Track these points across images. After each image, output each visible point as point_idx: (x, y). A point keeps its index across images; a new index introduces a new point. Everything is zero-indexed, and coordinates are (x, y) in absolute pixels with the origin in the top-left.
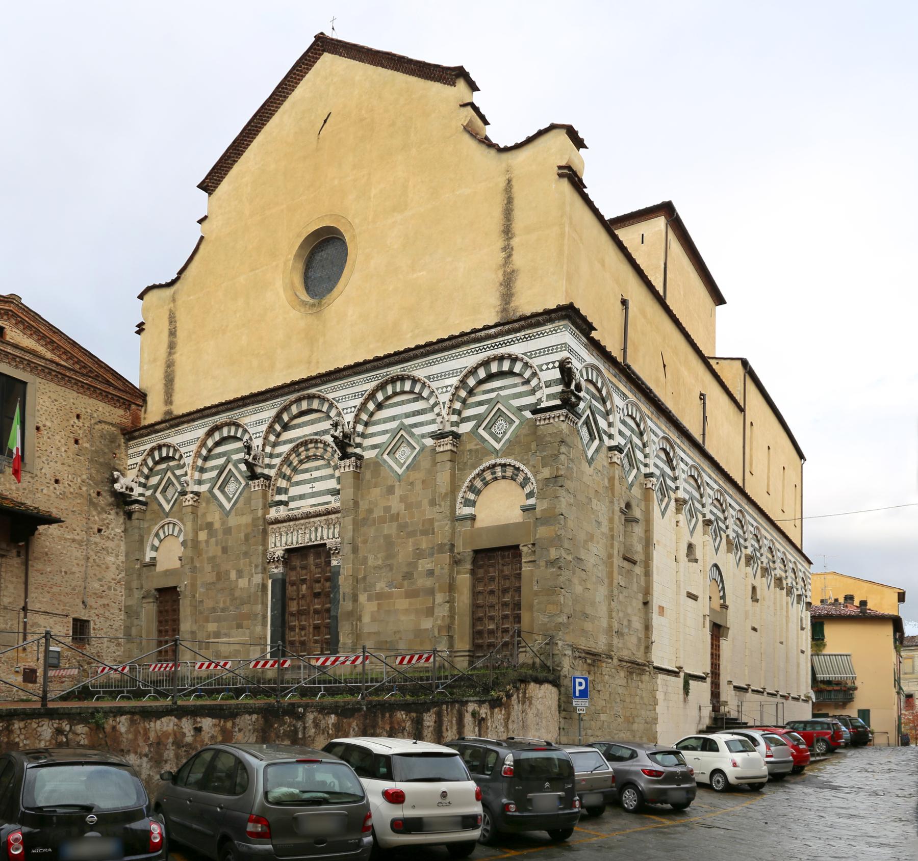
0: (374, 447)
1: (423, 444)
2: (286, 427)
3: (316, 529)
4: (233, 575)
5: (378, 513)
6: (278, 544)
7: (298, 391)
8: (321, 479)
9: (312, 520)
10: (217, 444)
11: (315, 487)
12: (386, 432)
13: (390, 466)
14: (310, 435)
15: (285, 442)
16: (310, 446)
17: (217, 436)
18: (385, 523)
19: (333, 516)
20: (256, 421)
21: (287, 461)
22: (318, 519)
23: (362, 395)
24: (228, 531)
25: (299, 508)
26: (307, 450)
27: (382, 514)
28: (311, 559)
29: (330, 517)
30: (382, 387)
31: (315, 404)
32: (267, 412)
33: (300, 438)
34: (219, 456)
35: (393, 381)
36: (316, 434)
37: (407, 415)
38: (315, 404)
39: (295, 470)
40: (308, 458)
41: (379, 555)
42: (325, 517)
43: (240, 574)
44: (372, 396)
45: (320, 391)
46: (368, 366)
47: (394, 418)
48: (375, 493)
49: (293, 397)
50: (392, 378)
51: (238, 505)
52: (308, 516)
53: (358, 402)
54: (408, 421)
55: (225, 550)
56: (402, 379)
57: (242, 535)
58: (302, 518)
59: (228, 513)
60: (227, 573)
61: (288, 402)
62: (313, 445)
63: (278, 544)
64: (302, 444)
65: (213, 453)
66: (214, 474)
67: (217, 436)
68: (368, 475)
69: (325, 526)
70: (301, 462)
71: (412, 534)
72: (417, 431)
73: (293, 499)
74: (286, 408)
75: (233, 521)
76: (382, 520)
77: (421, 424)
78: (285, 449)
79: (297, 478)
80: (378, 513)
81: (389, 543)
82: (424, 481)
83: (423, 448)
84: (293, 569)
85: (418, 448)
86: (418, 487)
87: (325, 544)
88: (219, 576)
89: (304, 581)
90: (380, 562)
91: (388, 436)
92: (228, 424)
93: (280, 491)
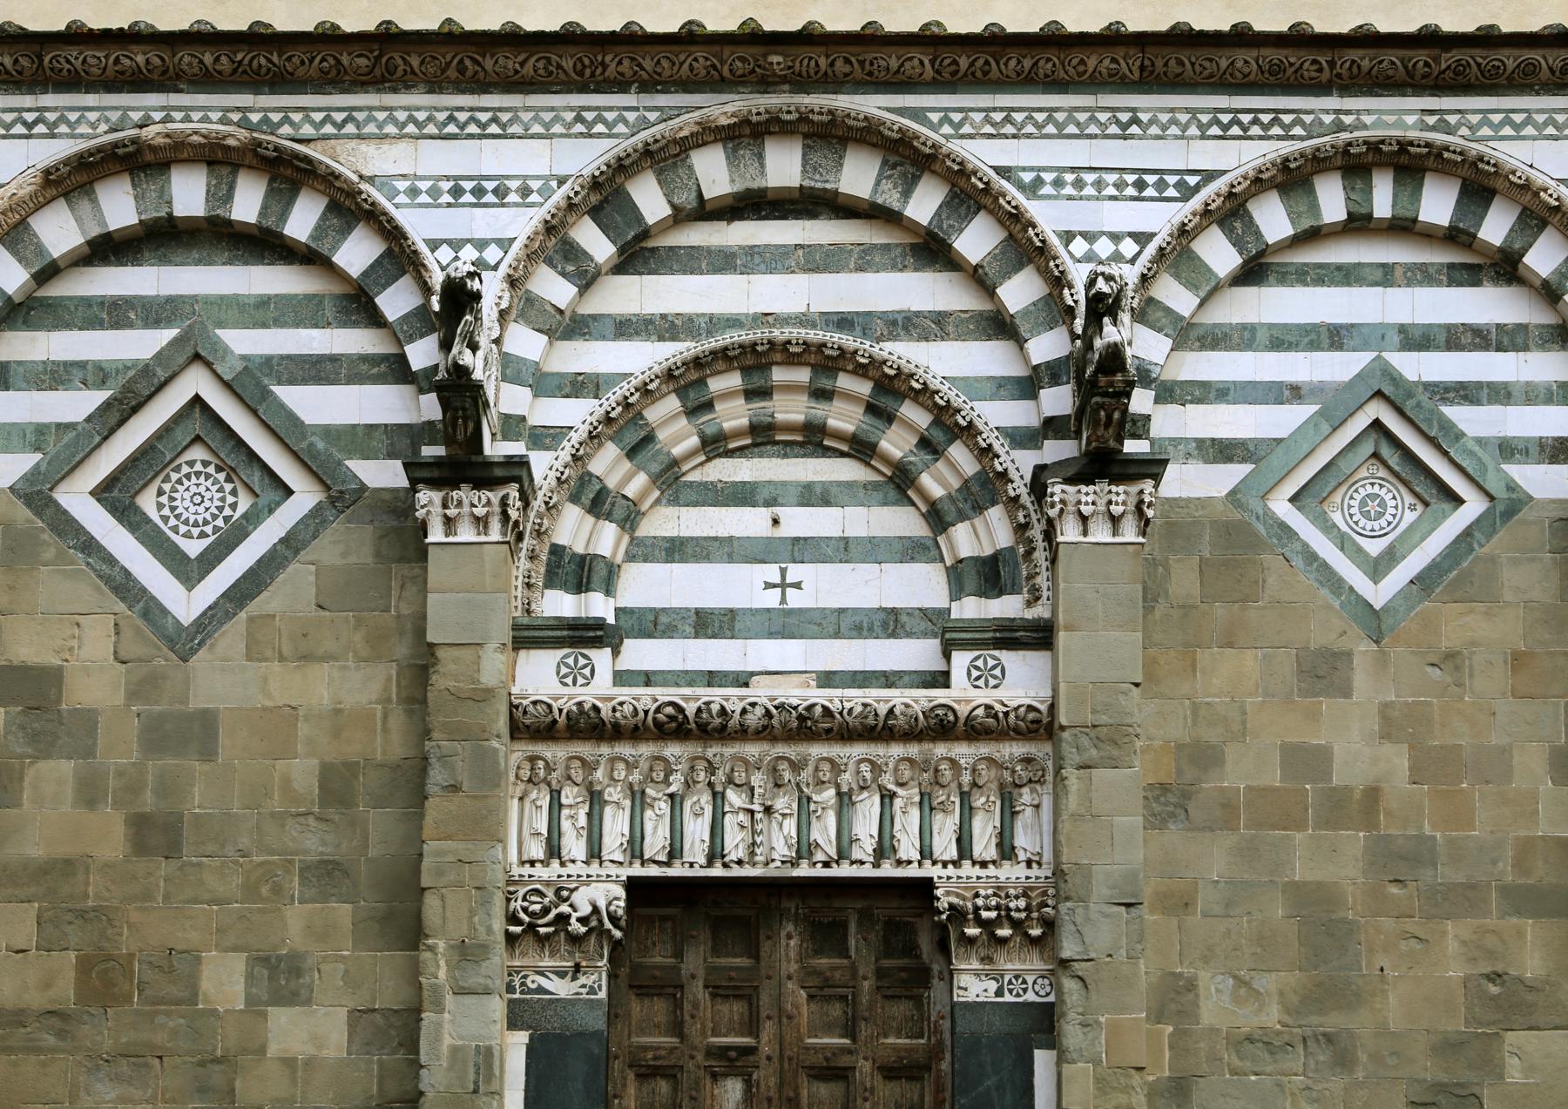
0: (1222, 451)
1: (1512, 487)
2: (638, 254)
3: (845, 800)
4: (225, 981)
5: (1247, 770)
6: (574, 846)
7: (766, 83)
8: (843, 550)
9: (817, 750)
10: (108, 249)
11: (786, 591)
12: (1294, 393)
13: (1311, 557)
14: (804, 320)
15: (625, 328)
16: (844, 382)
17: (119, 207)
18: (1300, 826)
19: (963, 751)
20: (469, 186)
21: (626, 426)
22: (858, 750)
23: (1187, 193)
24: (197, 733)
25: (742, 680)
26: (822, 395)
27: (1274, 777)
28: (788, 947)
29: (940, 750)
30: (1291, 179)
31: (858, 176)
32: (552, 149)
33: (733, 322)
34: (116, 313)
35: (1354, 165)
36: (844, 322)
37: (1417, 339)
38: (858, 176)
39: (671, 482)
40: (763, 436)
41: (1266, 982)
42: (913, 750)
43: (281, 979)
44: (1231, 213)
45: (918, 114)
46: (1245, 59)
47: (1334, 337)
48: (1232, 674)
49: (723, 107)
50: (1374, 146)
51: (264, 603)
52: (806, 726)
53: (1161, 218)
54: (1418, 367)
55: (156, 835)
56: (1411, 163)
57: (303, 772)
58: (765, 733)
59: (187, 641)
60: (178, 966)
61: (685, 125)
62: (803, 375)
63: (585, 848)
64: (724, 358)
65: (61, 289)
66: (78, 405)
67: (119, 207)
68: (1184, 581)
69: (907, 796)
70: (715, 445)
71: (1462, 899)
72: (1471, 420)
73: (653, 624)
74: (664, 157)
75: (219, 681)
76: (1275, 811)
77: (1500, 394)
78: (640, 358)
79: (665, 522)
80: (1247, 770)
81: (1321, 923)
82: (1518, 660)
83: (1508, 507)
84: (668, 987)
85: (1474, 506)
86: (1489, 680)
87: (927, 884)
88: (102, 979)
89: (733, 1062)
90: (1272, 1016)
91: (1301, 413)
92: (221, 160)
93: (579, 572)
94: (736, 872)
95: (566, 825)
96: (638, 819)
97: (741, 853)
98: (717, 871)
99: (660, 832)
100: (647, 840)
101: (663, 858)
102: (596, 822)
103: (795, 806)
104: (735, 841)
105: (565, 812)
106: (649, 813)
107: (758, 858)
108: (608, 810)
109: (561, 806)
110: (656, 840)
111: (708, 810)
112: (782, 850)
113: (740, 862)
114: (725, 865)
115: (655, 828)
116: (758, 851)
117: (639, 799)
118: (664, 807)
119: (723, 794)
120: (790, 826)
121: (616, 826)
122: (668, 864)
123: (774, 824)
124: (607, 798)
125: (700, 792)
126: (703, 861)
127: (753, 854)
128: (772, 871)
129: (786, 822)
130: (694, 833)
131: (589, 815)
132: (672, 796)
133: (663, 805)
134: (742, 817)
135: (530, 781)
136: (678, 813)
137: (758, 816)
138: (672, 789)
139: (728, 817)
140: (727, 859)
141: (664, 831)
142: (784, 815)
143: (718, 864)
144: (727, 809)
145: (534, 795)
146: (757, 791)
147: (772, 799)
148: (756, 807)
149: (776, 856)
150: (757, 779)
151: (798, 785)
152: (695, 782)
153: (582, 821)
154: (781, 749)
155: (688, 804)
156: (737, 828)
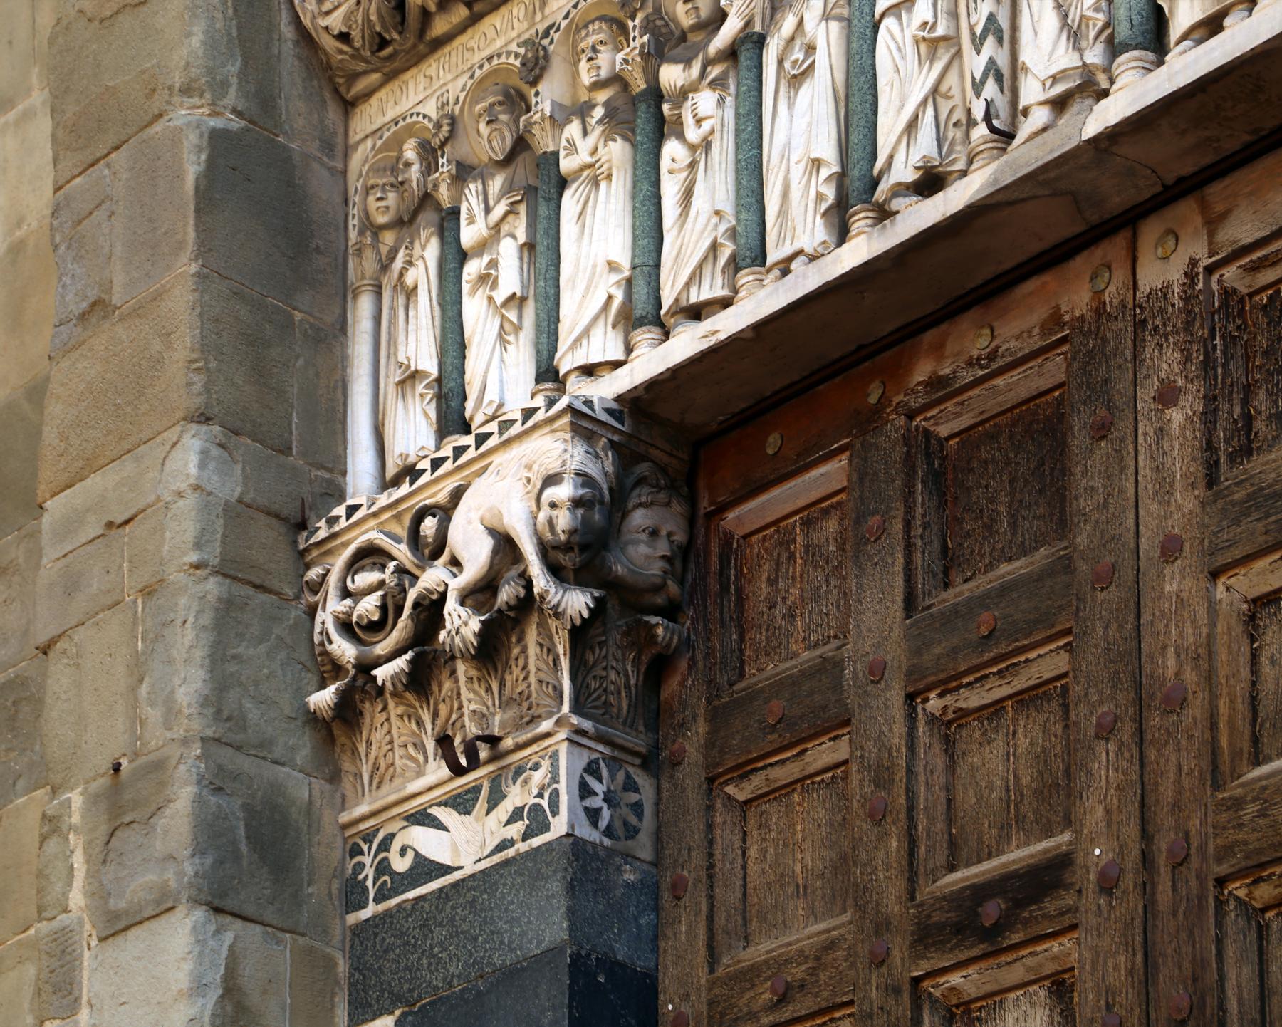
143: (860, 221)
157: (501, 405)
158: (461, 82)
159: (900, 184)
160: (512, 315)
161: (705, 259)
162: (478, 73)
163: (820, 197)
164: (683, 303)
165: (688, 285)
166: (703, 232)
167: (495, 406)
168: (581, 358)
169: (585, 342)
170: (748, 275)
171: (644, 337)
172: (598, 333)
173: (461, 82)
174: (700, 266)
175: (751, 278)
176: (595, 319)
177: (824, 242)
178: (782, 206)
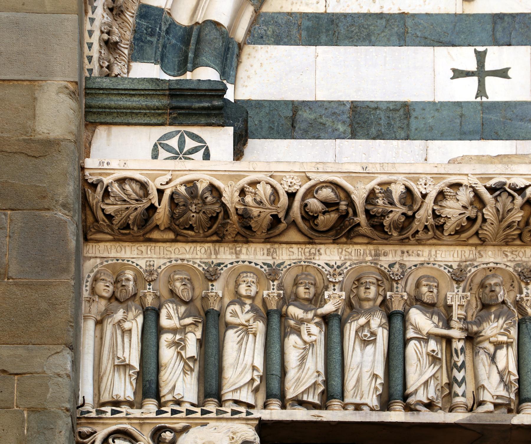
6: (180, 383)
94: (426, 417)
95: (167, 354)
96: (276, 348)
97: (432, 393)
98: (397, 415)
99: (310, 363)
100: (292, 374)
101: (315, 399)
102: (212, 351)
103: (514, 332)
104: (421, 374)
105: (166, 338)
106: (292, 340)
107: (459, 400)
108: (232, 338)
109: (160, 330)
110: (304, 372)
111: (382, 335)
112: (493, 389)
113: (430, 406)
114: (408, 408)
115: (303, 359)
116: (459, 390)
117: (276, 323)
118: (315, 332)
119: (404, 316)
120: (507, 359)
121: (242, 359)
122: (324, 406)
123: (483, 358)
124: (229, 318)
125: (370, 312)
126: (374, 402)
127: (451, 395)
128: (485, 415)
129: (501, 354)
130: (360, 365)
131: (201, 343)
132: (326, 319)
133: (315, 330)
134: (433, 345)
135: (113, 298)
136: (336, 339)
137: (458, 345)
138: (328, 308)
139: (412, 347)
140: (412, 400)
141: (316, 362)
142: (498, 346)
143: (398, 406)
144: (410, 333)
145: (120, 315)
146: (457, 312)
147: (479, 322)
148: (455, 333)
149: (486, 396)
150: (456, 297)
151: (518, 304)
152: (360, 300)
153: (192, 349)
154: (491, 256)
155: (351, 329)
156: (425, 360)
157: (183, 397)
158: (162, 261)
159: (421, 401)
160: (191, 364)
161: (310, 387)
162: (174, 262)
163: (376, 389)
164: (300, 398)
165: (303, 393)
166: (311, 376)
167: (181, 396)
168: (236, 397)
169: (239, 391)
170: (338, 402)
171: (275, 404)
172: (244, 391)
173: (162, 261)
174: (308, 388)
175: (339, 404)
176: (245, 385)
177: (376, 406)
178: (356, 384)
